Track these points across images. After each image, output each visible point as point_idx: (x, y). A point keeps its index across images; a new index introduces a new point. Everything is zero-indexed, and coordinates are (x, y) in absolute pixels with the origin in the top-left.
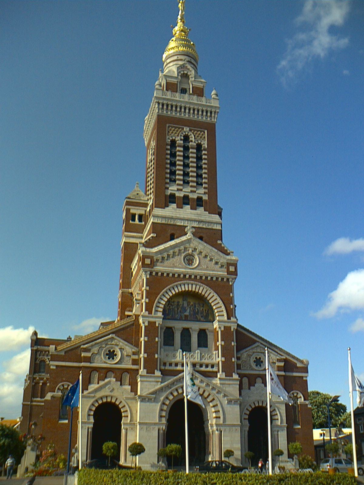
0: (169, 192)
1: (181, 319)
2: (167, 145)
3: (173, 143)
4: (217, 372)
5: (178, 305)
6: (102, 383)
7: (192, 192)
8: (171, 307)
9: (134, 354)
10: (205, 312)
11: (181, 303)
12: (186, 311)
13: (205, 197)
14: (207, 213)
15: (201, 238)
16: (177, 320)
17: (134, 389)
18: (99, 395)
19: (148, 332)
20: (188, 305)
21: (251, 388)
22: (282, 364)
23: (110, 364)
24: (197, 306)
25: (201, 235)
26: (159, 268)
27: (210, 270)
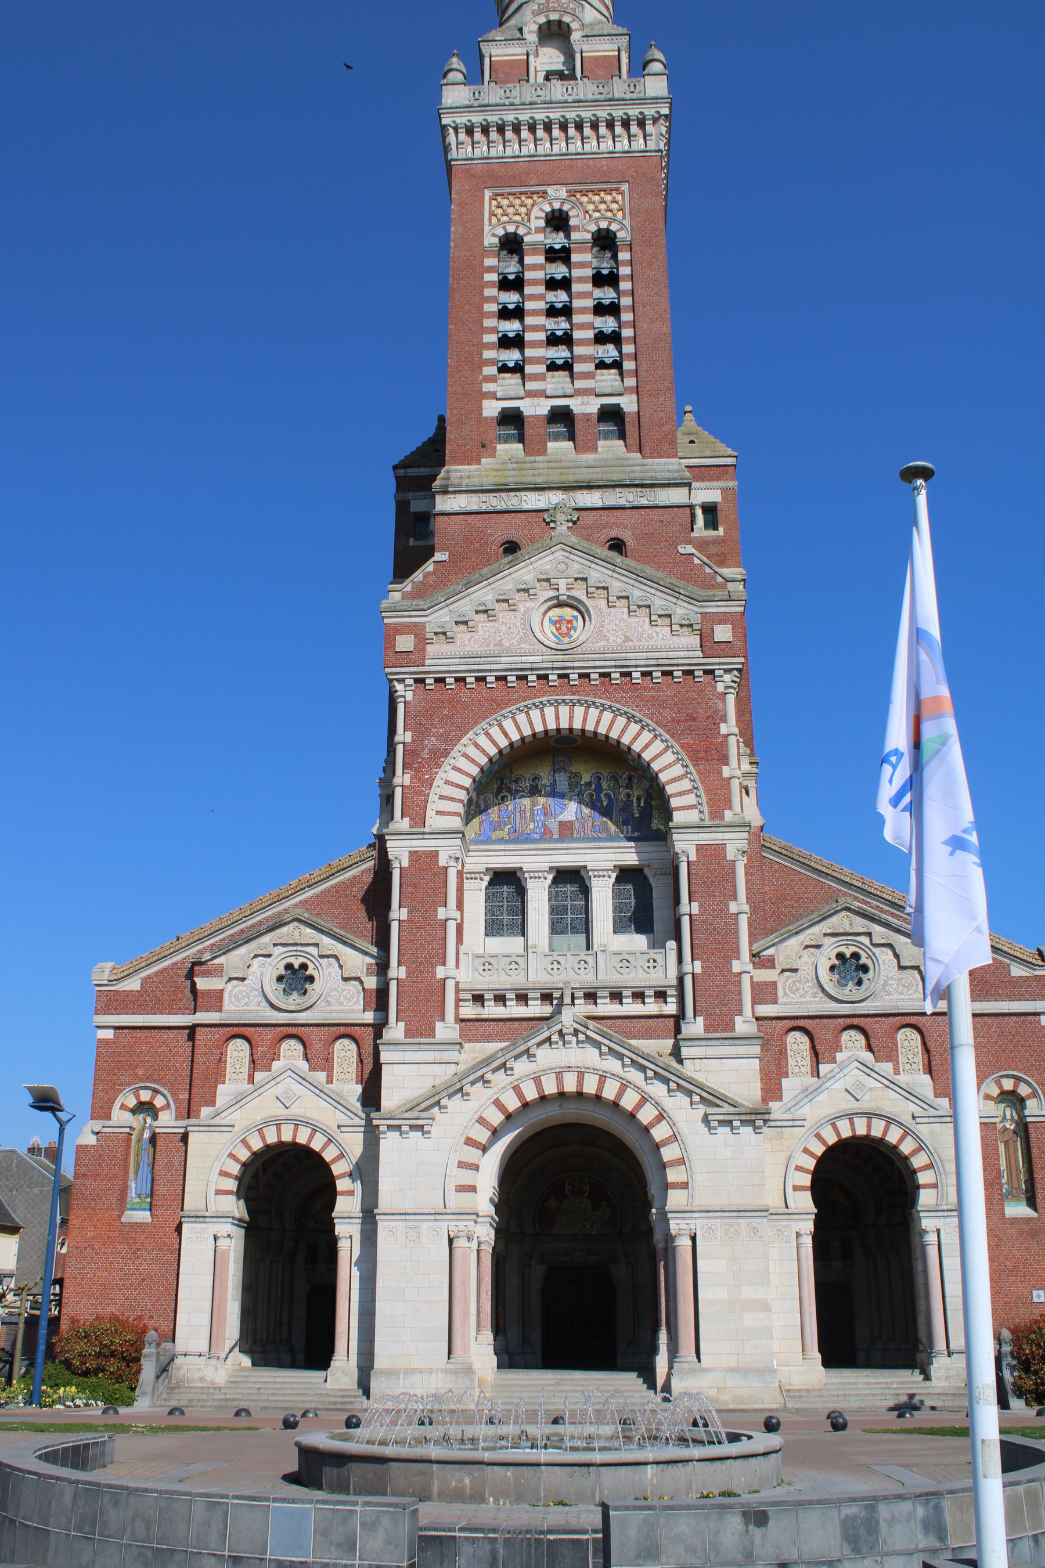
0: (491, 409)
1: (546, 836)
2: (486, 253)
3: (512, 245)
6: (259, 1076)
10: (639, 805)
11: (545, 781)
13: (628, 404)
15: (617, 546)
16: (533, 841)
17: (371, 1097)
18: (242, 1118)
19: (410, 889)
21: (824, 1068)
24: (604, 785)
25: (614, 533)
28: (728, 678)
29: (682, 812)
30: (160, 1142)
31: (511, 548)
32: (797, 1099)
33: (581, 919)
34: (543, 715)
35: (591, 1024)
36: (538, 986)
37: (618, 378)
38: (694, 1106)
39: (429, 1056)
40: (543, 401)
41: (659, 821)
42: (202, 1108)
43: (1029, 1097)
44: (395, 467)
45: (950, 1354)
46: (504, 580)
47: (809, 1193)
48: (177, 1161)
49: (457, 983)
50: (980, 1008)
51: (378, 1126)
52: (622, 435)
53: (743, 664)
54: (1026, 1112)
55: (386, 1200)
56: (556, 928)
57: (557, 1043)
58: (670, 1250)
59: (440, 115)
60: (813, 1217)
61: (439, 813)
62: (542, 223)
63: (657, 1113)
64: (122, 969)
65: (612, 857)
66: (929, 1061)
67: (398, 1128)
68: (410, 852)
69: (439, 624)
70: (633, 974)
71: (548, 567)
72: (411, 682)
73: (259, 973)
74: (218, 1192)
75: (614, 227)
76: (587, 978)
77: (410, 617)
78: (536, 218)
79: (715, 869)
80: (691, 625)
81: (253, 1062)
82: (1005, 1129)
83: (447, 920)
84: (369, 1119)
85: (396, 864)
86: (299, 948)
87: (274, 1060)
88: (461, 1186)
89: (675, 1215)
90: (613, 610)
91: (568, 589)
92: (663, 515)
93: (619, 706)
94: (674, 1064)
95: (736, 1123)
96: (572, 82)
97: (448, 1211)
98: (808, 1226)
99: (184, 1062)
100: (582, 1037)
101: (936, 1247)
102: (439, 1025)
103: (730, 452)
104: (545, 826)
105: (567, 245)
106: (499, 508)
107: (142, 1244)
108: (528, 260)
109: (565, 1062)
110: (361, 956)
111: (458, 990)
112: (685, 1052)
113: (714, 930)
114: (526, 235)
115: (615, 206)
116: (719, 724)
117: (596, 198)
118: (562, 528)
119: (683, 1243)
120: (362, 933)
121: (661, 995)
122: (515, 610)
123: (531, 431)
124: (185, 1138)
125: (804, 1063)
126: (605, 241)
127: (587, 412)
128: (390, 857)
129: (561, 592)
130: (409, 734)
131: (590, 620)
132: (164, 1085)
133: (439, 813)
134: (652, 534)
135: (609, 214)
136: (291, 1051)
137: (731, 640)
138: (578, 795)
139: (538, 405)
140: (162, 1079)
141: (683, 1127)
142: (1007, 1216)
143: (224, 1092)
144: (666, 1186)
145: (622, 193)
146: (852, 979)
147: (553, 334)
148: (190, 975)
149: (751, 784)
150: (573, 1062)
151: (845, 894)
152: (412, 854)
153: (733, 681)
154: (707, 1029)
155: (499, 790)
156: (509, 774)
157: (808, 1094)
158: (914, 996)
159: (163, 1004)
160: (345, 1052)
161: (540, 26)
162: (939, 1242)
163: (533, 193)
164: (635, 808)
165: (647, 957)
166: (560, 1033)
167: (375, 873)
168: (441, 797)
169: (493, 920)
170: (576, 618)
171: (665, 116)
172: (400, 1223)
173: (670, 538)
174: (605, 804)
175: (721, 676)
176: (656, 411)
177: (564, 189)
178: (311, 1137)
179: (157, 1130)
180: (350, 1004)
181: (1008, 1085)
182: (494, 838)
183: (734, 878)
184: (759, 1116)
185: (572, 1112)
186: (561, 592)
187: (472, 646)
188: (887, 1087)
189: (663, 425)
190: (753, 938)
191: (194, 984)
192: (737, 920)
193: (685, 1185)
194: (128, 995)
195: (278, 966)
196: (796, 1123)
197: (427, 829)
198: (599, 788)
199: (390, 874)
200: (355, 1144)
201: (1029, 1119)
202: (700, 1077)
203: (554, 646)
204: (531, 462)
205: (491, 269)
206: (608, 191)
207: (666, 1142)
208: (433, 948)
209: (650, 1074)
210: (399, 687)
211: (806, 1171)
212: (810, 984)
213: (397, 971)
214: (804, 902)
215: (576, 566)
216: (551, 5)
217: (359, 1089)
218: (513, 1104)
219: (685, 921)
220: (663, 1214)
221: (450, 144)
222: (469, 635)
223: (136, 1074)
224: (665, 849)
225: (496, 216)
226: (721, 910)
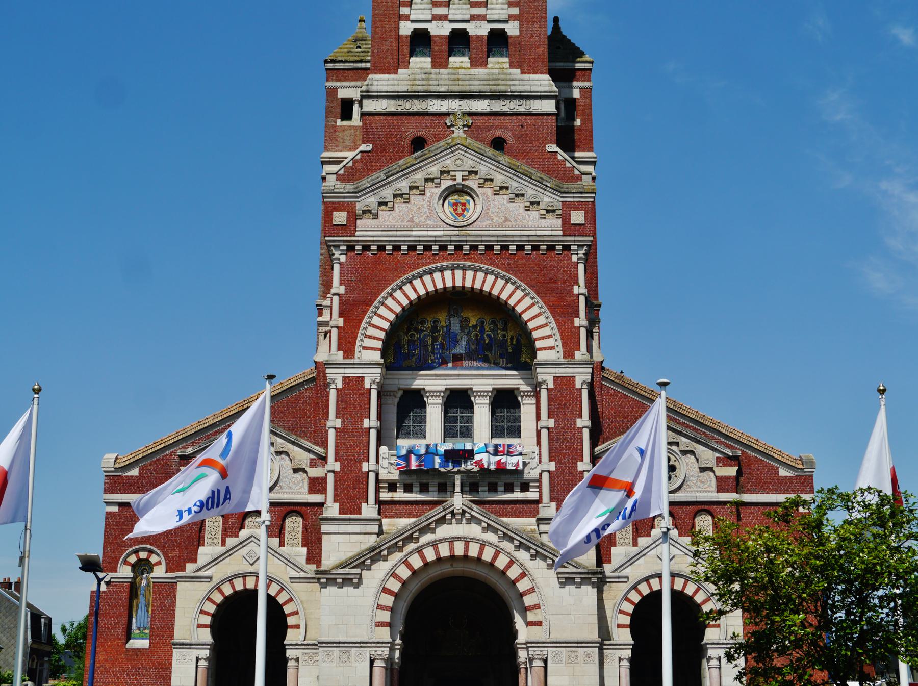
0: (406, 29)
4: (537, 502)
5: (435, 329)
6: (231, 541)
7: (474, 18)
8: (416, 336)
9: (313, 464)
10: (512, 343)
12: (456, 342)
13: (512, 29)
14: (519, 71)
15: (498, 144)
17: (314, 556)
18: (218, 573)
19: (343, 405)
20: (462, 329)
22: (732, 471)
24: (487, 328)
25: (497, 134)
26: (366, 230)
29: (544, 352)
31: (419, 143)
34: (443, 276)
35: (475, 507)
40: (446, 24)
41: (527, 356)
42: (187, 564)
47: (628, 630)
50: (756, 498)
53: (592, 241)
63: (521, 571)
64: (124, 459)
65: (492, 382)
68: (343, 377)
69: (365, 204)
77: (344, 198)
79: (567, 395)
80: (554, 211)
83: (370, 428)
87: (240, 529)
88: (379, 622)
90: (496, 196)
91: (463, 180)
92: (535, 120)
93: (500, 271)
98: (627, 653)
100: (467, 516)
102: (364, 505)
107: (142, 664)
109: (455, 534)
111: (378, 481)
113: (565, 439)
116: (573, 286)
118: (459, 133)
120: (306, 435)
122: (423, 195)
123: (436, 48)
124: (173, 585)
127: (479, 34)
131: (478, 196)
132: (157, 547)
137: (584, 223)
138: (467, 334)
140: (156, 542)
143: (205, 553)
155: (409, 330)
157: (631, 561)
158: (708, 489)
164: (509, 345)
173: (540, 138)
174: (487, 342)
176: (533, 36)
180: (297, 488)
185: (459, 568)
187: (390, 222)
188: (687, 555)
189: (538, 48)
192: (582, 432)
194: (129, 479)
197: (356, 360)
198: (483, 330)
204: (436, 74)
210: (337, 254)
211: (627, 614)
214: (631, 419)
215: (470, 162)
219: (544, 433)
222: (389, 213)
224: (530, 377)
226: (571, 425)
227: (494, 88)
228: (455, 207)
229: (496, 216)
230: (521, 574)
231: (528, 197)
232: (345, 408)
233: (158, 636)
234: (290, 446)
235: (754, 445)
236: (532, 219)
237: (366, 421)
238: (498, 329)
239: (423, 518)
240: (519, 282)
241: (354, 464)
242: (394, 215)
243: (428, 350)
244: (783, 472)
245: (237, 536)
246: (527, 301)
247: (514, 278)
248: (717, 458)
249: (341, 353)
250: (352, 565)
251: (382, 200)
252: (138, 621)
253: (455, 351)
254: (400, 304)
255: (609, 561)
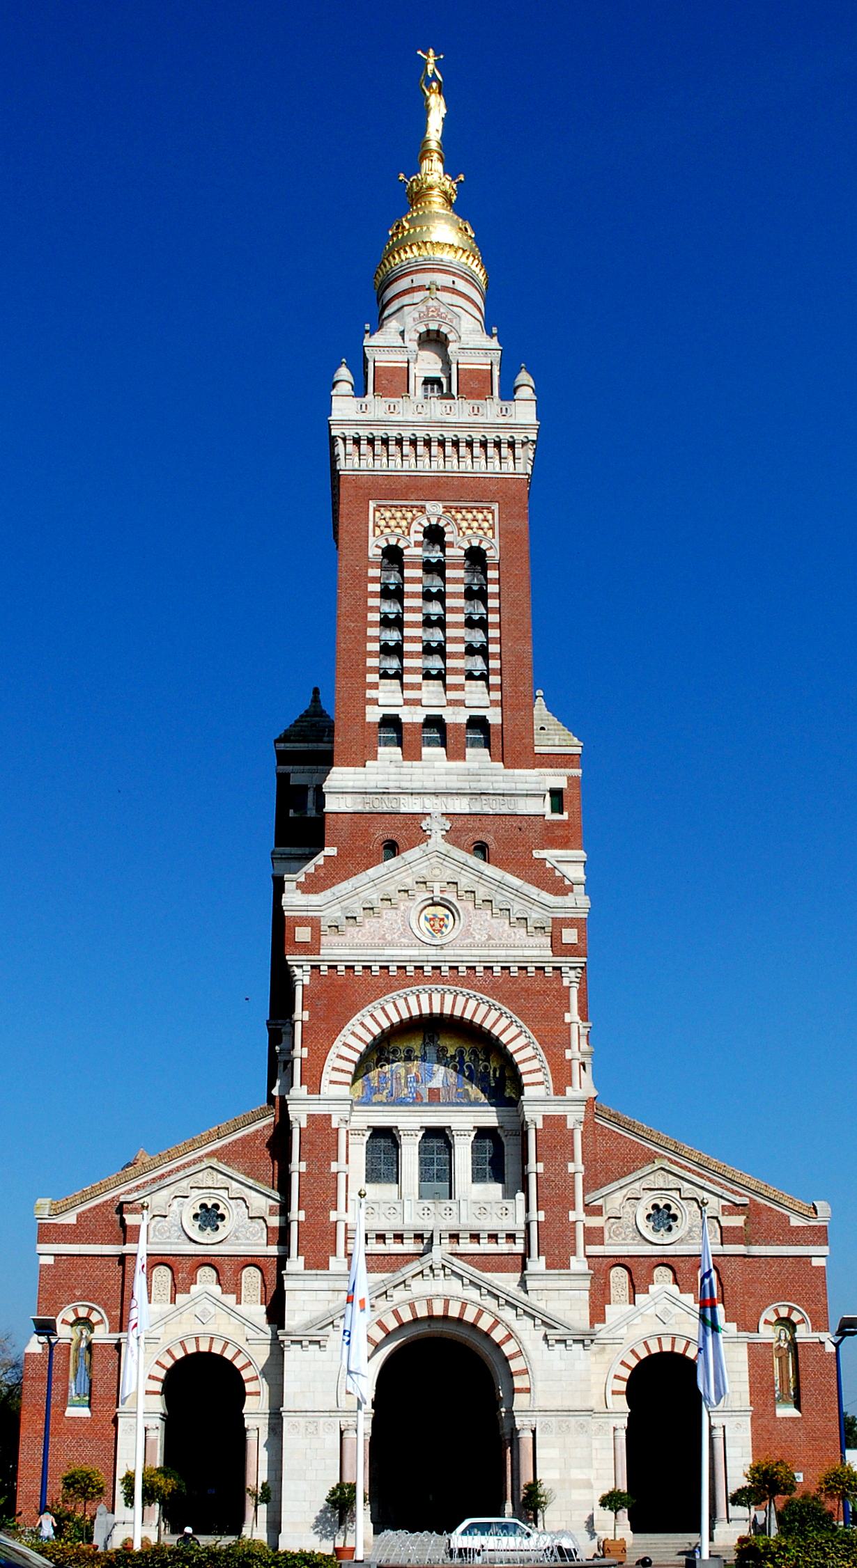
0: (374, 715)
1: (417, 1101)
3: (393, 555)
13: (494, 717)
15: (481, 849)
16: (407, 1104)
19: (308, 1147)
22: (738, 1221)
23: (208, 1242)
24: (467, 1058)
26: (335, 950)
27: (496, 947)
28: (572, 973)
29: (531, 1087)
30: (96, 1351)
31: (392, 848)
32: (619, 1321)
33: (445, 1170)
35: (454, 1260)
36: (412, 1228)
37: (486, 691)
38: (536, 1328)
39: (324, 1284)
43: (799, 1322)
44: (276, 741)
45: (729, 1521)
46: (387, 882)
48: (112, 1364)
49: (346, 1224)
51: (283, 1341)
52: (487, 745)
53: (585, 963)
54: (797, 1335)
55: (290, 1401)
56: (424, 1176)
57: (428, 1275)
58: (515, 1440)
59: (330, 425)
60: (627, 1415)
61: (332, 1082)
62: (420, 537)
63: (507, 1333)
65: (472, 1119)
66: (723, 1293)
67: (300, 1342)
68: (308, 1115)
70: (488, 1220)
71: (424, 872)
72: (309, 968)
73: (178, 1212)
74: (147, 1393)
75: (484, 546)
76: (451, 1223)
78: (416, 532)
79: (558, 1136)
80: (544, 928)
81: (175, 1285)
82: (780, 1347)
83: (338, 1173)
84: (275, 1338)
85: (295, 1125)
86: (212, 1191)
89: (520, 1413)
90: (479, 911)
92: (521, 822)
93: (482, 996)
94: (522, 1294)
95: (569, 1342)
96: (451, 401)
97: (340, 1410)
98: (623, 1422)
99: (115, 1284)
101: (722, 1440)
103: (576, 740)
104: (417, 1092)
105: (442, 559)
106: (380, 810)
107: (84, 1435)
108: (408, 573)
110: (264, 1199)
112: (530, 1285)
113: (556, 1185)
114: (406, 548)
115: (485, 525)
117: (469, 516)
118: (437, 841)
119: (526, 1436)
121: (511, 1237)
122: (396, 908)
123: (408, 737)
124: (118, 1347)
125: (624, 1293)
126: (476, 557)
127: (458, 722)
128: (291, 1119)
129: (435, 894)
130: (306, 1013)
132: (98, 1304)
133: (332, 1082)
134: (512, 839)
135: (481, 532)
136: (206, 1274)
139: (415, 713)
141: (528, 1346)
142: (778, 1416)
144: (513, 1391)
145: (492, 512)
146: (663, 1226)
147: (428, 645)
148: (120, 1209)
149: (588, 1060)
150: (440, 1291)
151: (661, 1156)
152: (309, 1116)
153: (577, 977)
154: (548, 1267)
155: (379, 1060)
156: (387, 1046)
159: (96, 1235)
160: (251, 1278)
161: (420, 334)
162: (724, 1435)
163: (413, 507)
165: (501, 1206)
166: (431, 1267)
167: (275, 1128)
168: (334, 1069)
169: (372, 1169)
170: (447, 916)
171: (533, 441)
172: (301, 1419)
175: (567, 973)
176: (517, 725)
177: (441, 505)
178: (225, 1348)
179: (94, 1341)
181: (784, 1313)
182: (374, 1101)
183: (572, 1144)
184: (587, 1337)
186: (435, 894)
190: (586, 1191)
191: (123, 1220)
192: (573, 1178)
193: (528, 1390)
195: (194, 1206)
196: (617, 1341)
197: (321, 1097)
199: (290, 1133)
200: (261, 1355)
201: (798, 1340)
202: (541, 1305)
203: (428, 941)
205: (375, 580)
206: (480, 510)
207: (513, 1356)
208: (327, 1196)
209: (502, 1302)
212: (631, 1230)
213: (297, 1215)
214: (628, 1162)
215: (449, 872)
216: (431, 314)
217: (264, 1308)
218: (392, 1324)
219: (532, 1178)
220: (510, 1412)
221: (338, 455)
222: (357, 929)
223: (74, 1294)
225: (379, 527)
227: (474, 785)
228: (432, 923)
229: (479, 934)
230: (507, 1336)
231: (515, 911)
232: (310, 1150)
233: (100, 1403)
234: (247, 1190)
235: (762, 1191)
236: (518, 937)
237: (333, 1164)
238: (479, 1060)
239: (399, 1274)
240: (505, 1009)
241: (320, 1212)
242: (364, 931)
243: (400, 1084)
244: (795, 1221)
245: (188, 1292)
246: (514, 1030)
247: (498, 1005)
248: (723, 1206)
249: (305, 1087)
250: (319, 1326)
251: (349, 915)
252: (78, 1386)
253: (430, 1085)
254: (372, 1033)
255: (604, 1321)
